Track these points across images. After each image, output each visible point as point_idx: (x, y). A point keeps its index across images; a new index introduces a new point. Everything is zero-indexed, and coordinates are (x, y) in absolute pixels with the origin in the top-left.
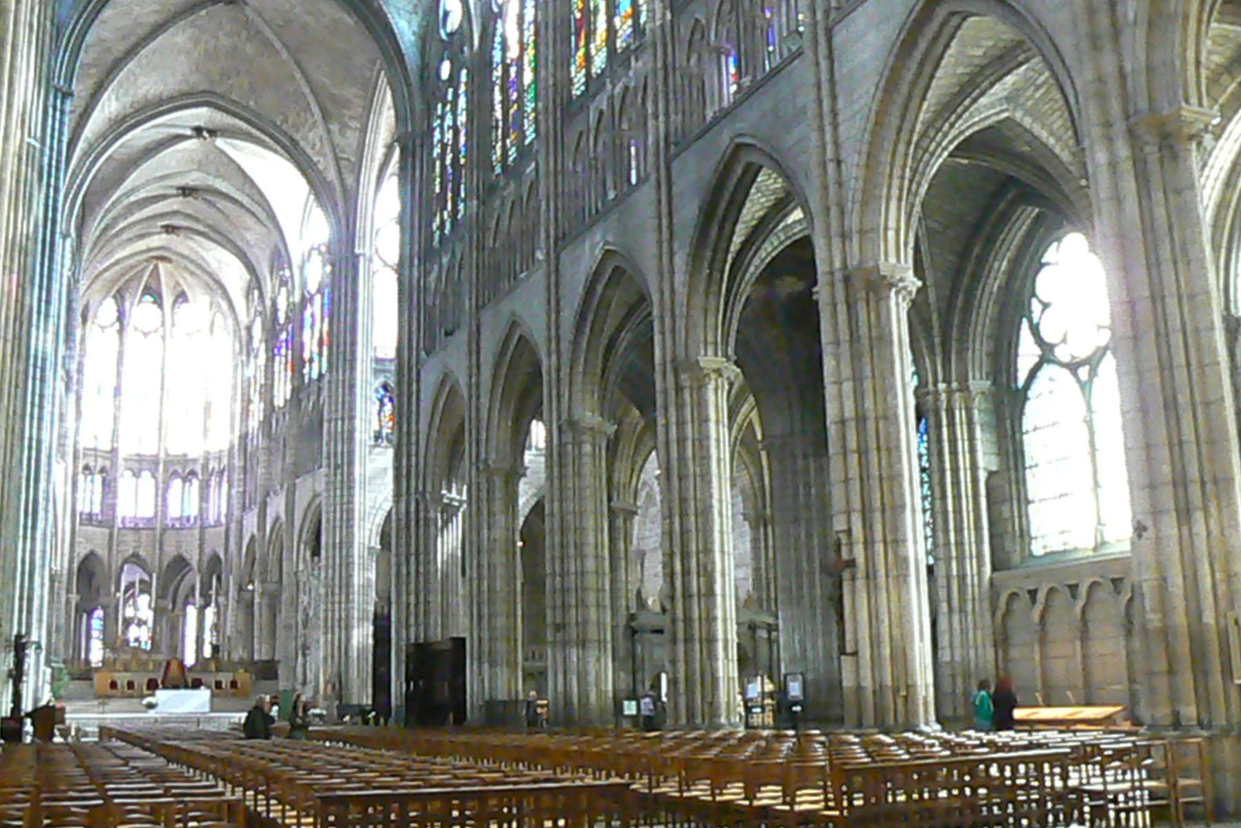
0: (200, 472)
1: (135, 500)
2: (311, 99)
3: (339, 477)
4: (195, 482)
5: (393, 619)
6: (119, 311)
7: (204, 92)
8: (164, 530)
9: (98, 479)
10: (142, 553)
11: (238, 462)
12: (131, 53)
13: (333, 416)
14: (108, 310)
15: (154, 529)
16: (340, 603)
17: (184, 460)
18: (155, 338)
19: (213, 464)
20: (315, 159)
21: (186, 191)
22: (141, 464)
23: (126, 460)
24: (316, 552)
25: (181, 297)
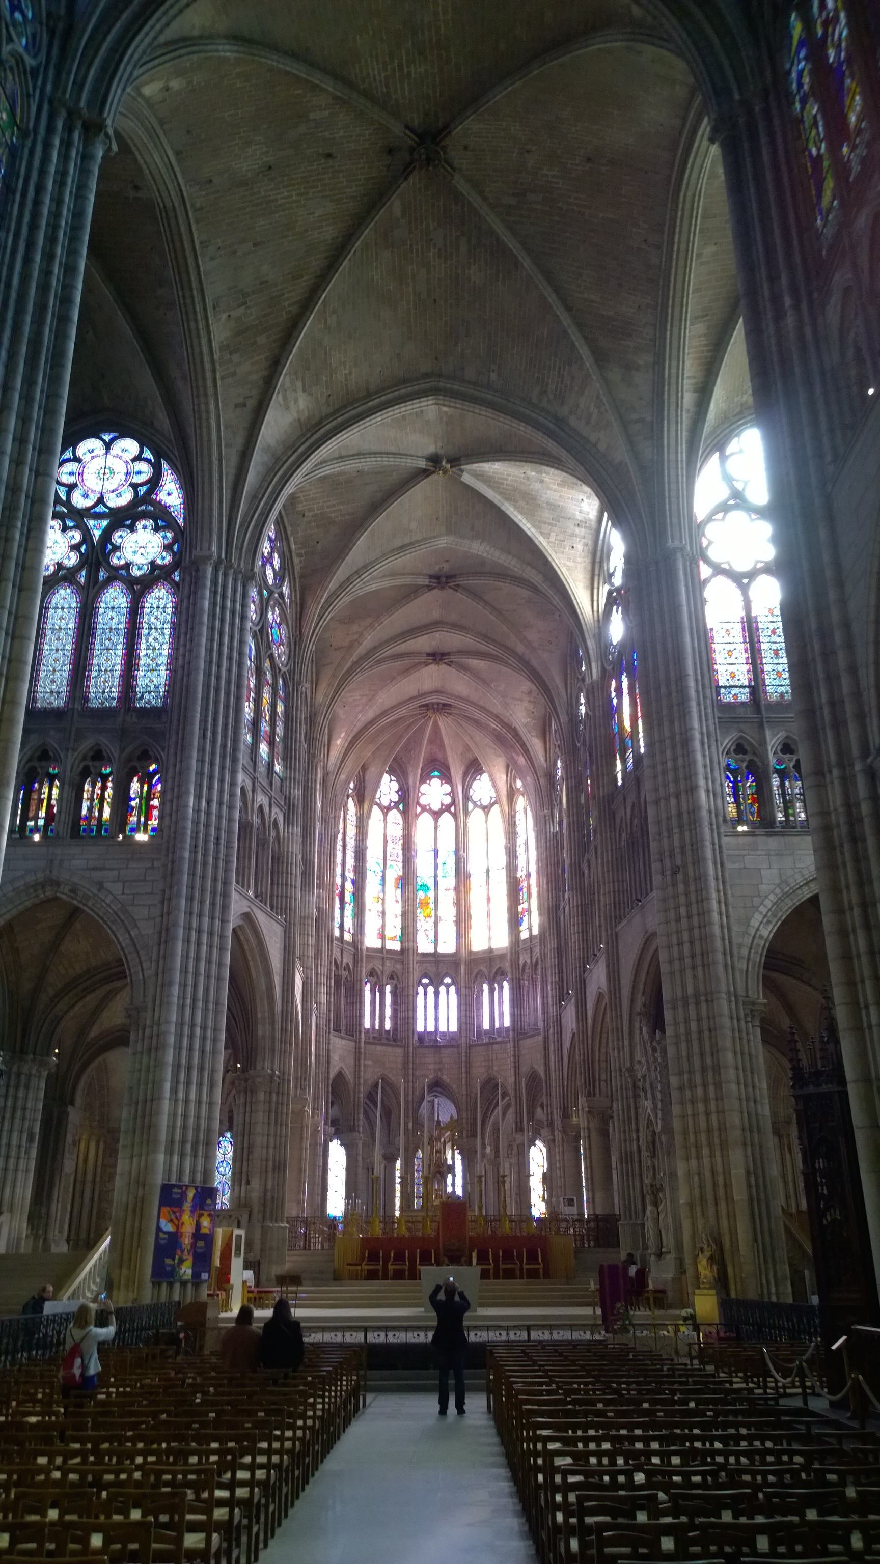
0: (508, 970)
1: (437, 1012)
2: (575, 335)
3: (681, 887)
4: (506, 984)
5: (850, 1073)
6: (401, 789)
7: (426, 375)
8: (470, 1047)
9: (388, 988)
10: (445, 1077)
11: (551, 944)
12: (307, 304)
13: (662, 793)
14: (388, 789)
15: (458, 1046)
16: (706, 1100)
17: (490, 957)
18: (446, 819)
19: (524, 958)
20: (593, 438)
21: (442, 580)
22: (438, 968)
23: (421, 962)
24: (657, 1022)
25: (473, 768)
